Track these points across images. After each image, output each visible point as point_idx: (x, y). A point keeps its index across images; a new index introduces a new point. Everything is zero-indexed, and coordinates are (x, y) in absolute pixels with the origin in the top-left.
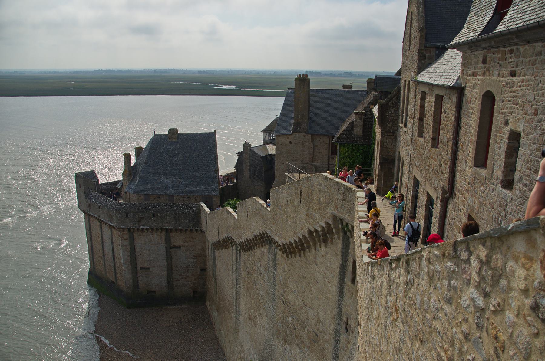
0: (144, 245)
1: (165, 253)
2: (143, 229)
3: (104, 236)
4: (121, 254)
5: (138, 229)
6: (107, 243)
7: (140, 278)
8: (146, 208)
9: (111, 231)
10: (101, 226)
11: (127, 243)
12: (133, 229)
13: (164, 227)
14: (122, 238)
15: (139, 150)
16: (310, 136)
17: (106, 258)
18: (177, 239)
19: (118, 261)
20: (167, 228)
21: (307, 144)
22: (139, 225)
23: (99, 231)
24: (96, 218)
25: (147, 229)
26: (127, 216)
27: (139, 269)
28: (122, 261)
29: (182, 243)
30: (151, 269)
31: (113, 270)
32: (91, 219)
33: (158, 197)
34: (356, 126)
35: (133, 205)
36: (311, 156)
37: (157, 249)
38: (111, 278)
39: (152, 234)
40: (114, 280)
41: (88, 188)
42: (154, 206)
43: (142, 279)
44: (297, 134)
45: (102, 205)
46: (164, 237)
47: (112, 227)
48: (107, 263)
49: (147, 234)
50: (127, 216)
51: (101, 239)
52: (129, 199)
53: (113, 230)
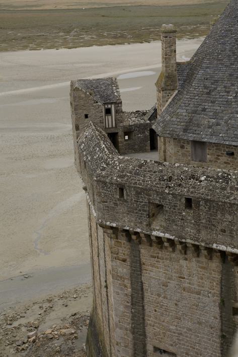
1: (217, 323)
8: (170, 179)
11: (124, 270)
12: (136, 233)
13: (215, 246)
14: (115, 256)
20: (223, 248)
22: (149, 225)
26: (122, 195)
27: (150, 348)
33: (227, 154)
35: (141, 166)
37: (197, 306)
39: (186, 259)
41: (86, 116)
42: (193, 177)
45: (87, 158)
46: (217, 276)
49: (173, 255)
50: (122, 195)
52: (165, 152)
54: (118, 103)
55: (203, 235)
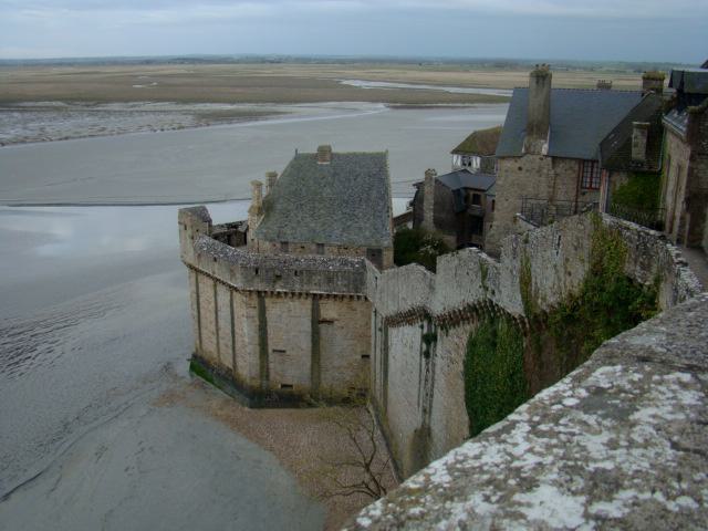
0: (280, 316)
1: (310, 329)
2: (279, 293)
3: (220, 304)
4: (247, 330)
5: (272, 292)
6: (225, 313)
7: (271, 366)
9: (232, 293)
10: (215, 286)
11: (255, 313)
12: (265, 292)
14: (248, 306)
15: (272, 176)
16: (549, 159)
17: (220, 332)
18: (329, 310)
19: (240, 339)
21: (545, 171)
23: (211, 293)
24: (208, 275)
25: (285, 293)
26: (257, 272)
27: (270, 351)
28: (247, 340)
29: (336, 316)
30: (288, 353)
31: (231, 351)
32: (200, 277)
34: (636, 146)
36: (551, 190)
38: (228, 363)
40: (231, 367)
43: (274, 363)
44: (531, 157)
47: (233, 289)
48: (221, 341)
50: (257, 272)
51: (213, 304)
53: (235, 293)
54: (210, 221)
55: (306, 287)
